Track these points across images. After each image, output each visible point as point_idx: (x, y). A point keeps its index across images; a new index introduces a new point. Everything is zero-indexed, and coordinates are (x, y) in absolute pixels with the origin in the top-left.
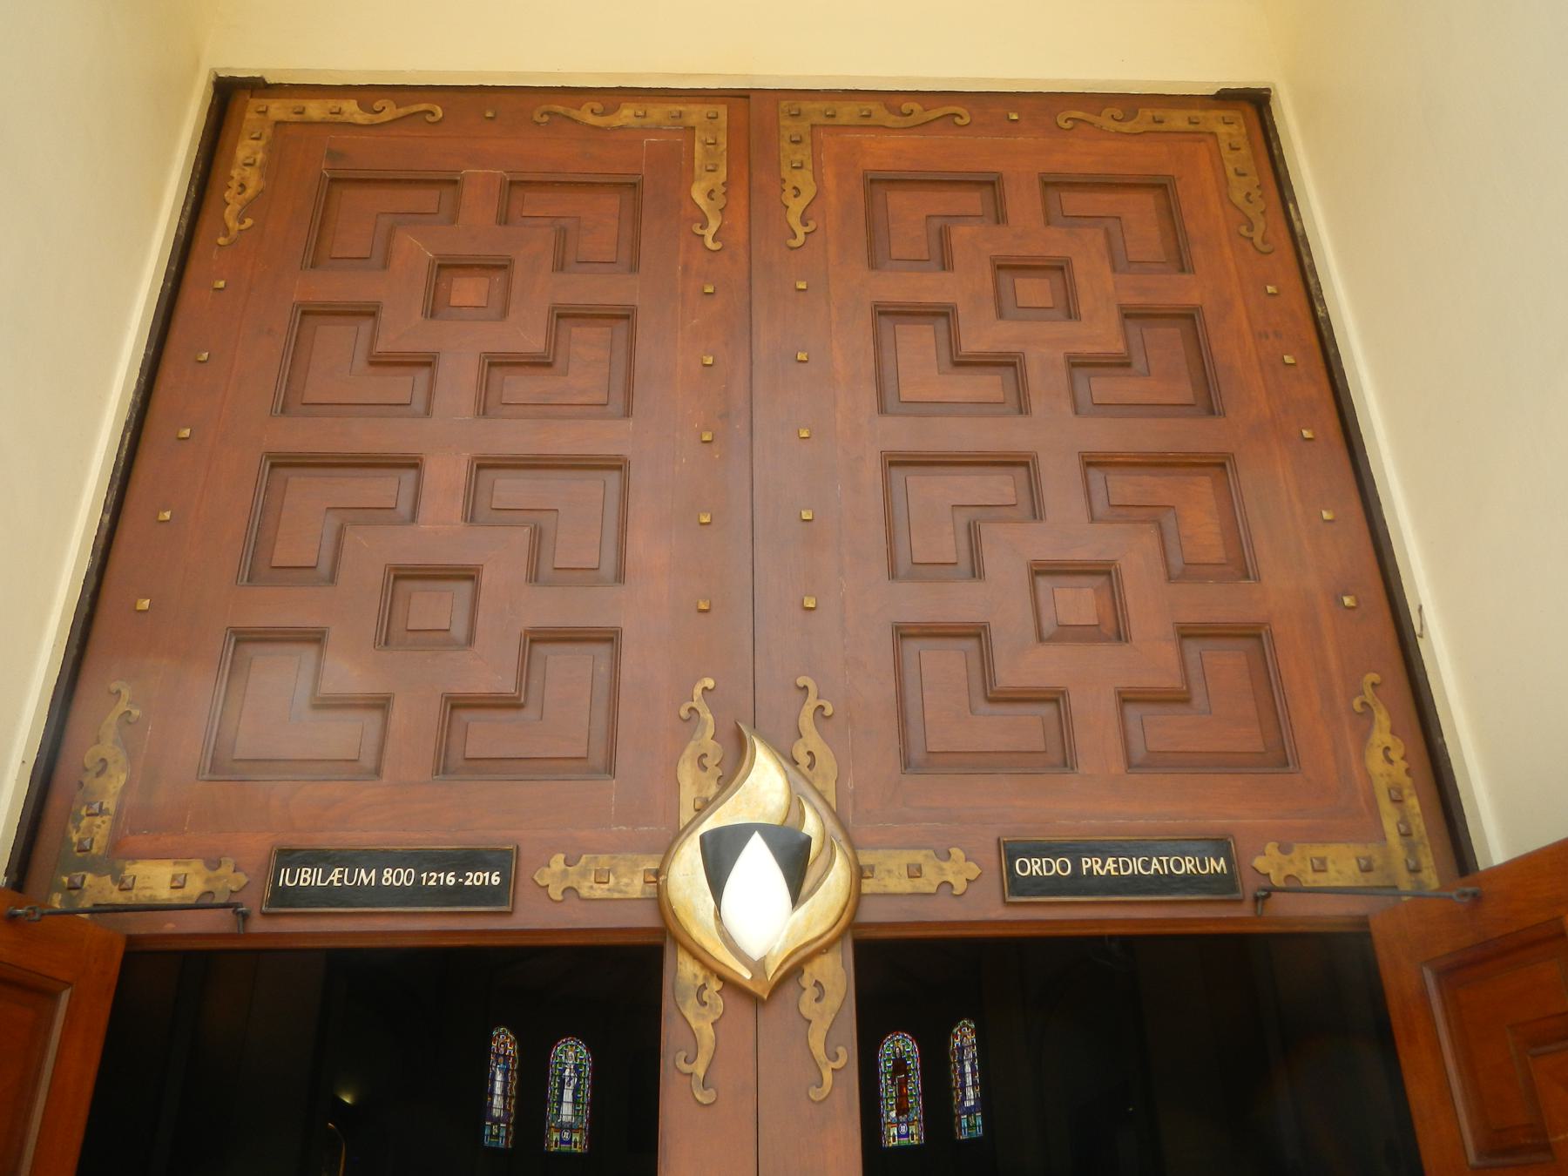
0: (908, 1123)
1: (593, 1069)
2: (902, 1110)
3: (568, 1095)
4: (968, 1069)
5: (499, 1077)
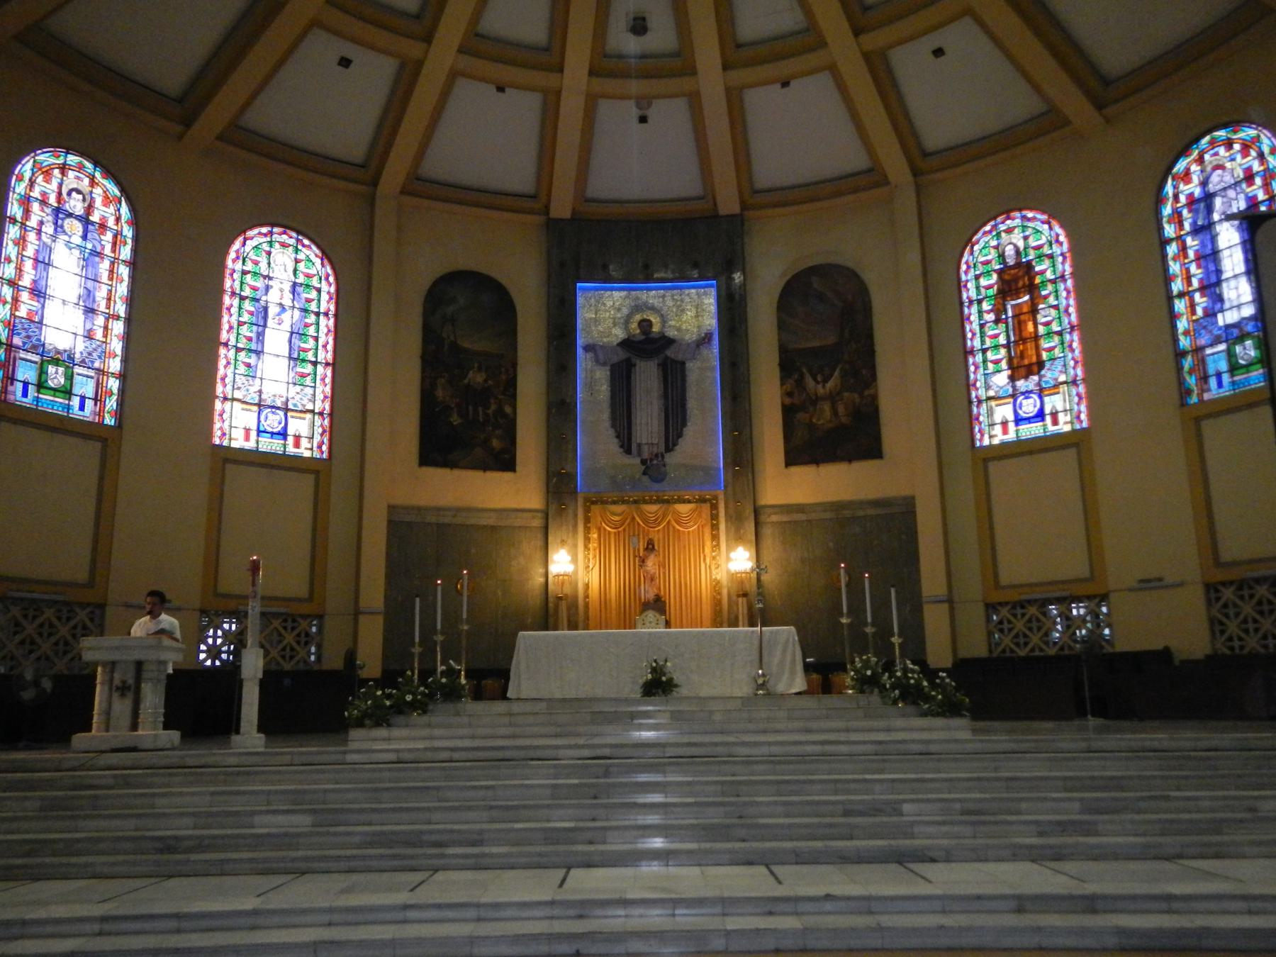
2: (1024, 363)
3: (276, 340)
5: (66, 260)
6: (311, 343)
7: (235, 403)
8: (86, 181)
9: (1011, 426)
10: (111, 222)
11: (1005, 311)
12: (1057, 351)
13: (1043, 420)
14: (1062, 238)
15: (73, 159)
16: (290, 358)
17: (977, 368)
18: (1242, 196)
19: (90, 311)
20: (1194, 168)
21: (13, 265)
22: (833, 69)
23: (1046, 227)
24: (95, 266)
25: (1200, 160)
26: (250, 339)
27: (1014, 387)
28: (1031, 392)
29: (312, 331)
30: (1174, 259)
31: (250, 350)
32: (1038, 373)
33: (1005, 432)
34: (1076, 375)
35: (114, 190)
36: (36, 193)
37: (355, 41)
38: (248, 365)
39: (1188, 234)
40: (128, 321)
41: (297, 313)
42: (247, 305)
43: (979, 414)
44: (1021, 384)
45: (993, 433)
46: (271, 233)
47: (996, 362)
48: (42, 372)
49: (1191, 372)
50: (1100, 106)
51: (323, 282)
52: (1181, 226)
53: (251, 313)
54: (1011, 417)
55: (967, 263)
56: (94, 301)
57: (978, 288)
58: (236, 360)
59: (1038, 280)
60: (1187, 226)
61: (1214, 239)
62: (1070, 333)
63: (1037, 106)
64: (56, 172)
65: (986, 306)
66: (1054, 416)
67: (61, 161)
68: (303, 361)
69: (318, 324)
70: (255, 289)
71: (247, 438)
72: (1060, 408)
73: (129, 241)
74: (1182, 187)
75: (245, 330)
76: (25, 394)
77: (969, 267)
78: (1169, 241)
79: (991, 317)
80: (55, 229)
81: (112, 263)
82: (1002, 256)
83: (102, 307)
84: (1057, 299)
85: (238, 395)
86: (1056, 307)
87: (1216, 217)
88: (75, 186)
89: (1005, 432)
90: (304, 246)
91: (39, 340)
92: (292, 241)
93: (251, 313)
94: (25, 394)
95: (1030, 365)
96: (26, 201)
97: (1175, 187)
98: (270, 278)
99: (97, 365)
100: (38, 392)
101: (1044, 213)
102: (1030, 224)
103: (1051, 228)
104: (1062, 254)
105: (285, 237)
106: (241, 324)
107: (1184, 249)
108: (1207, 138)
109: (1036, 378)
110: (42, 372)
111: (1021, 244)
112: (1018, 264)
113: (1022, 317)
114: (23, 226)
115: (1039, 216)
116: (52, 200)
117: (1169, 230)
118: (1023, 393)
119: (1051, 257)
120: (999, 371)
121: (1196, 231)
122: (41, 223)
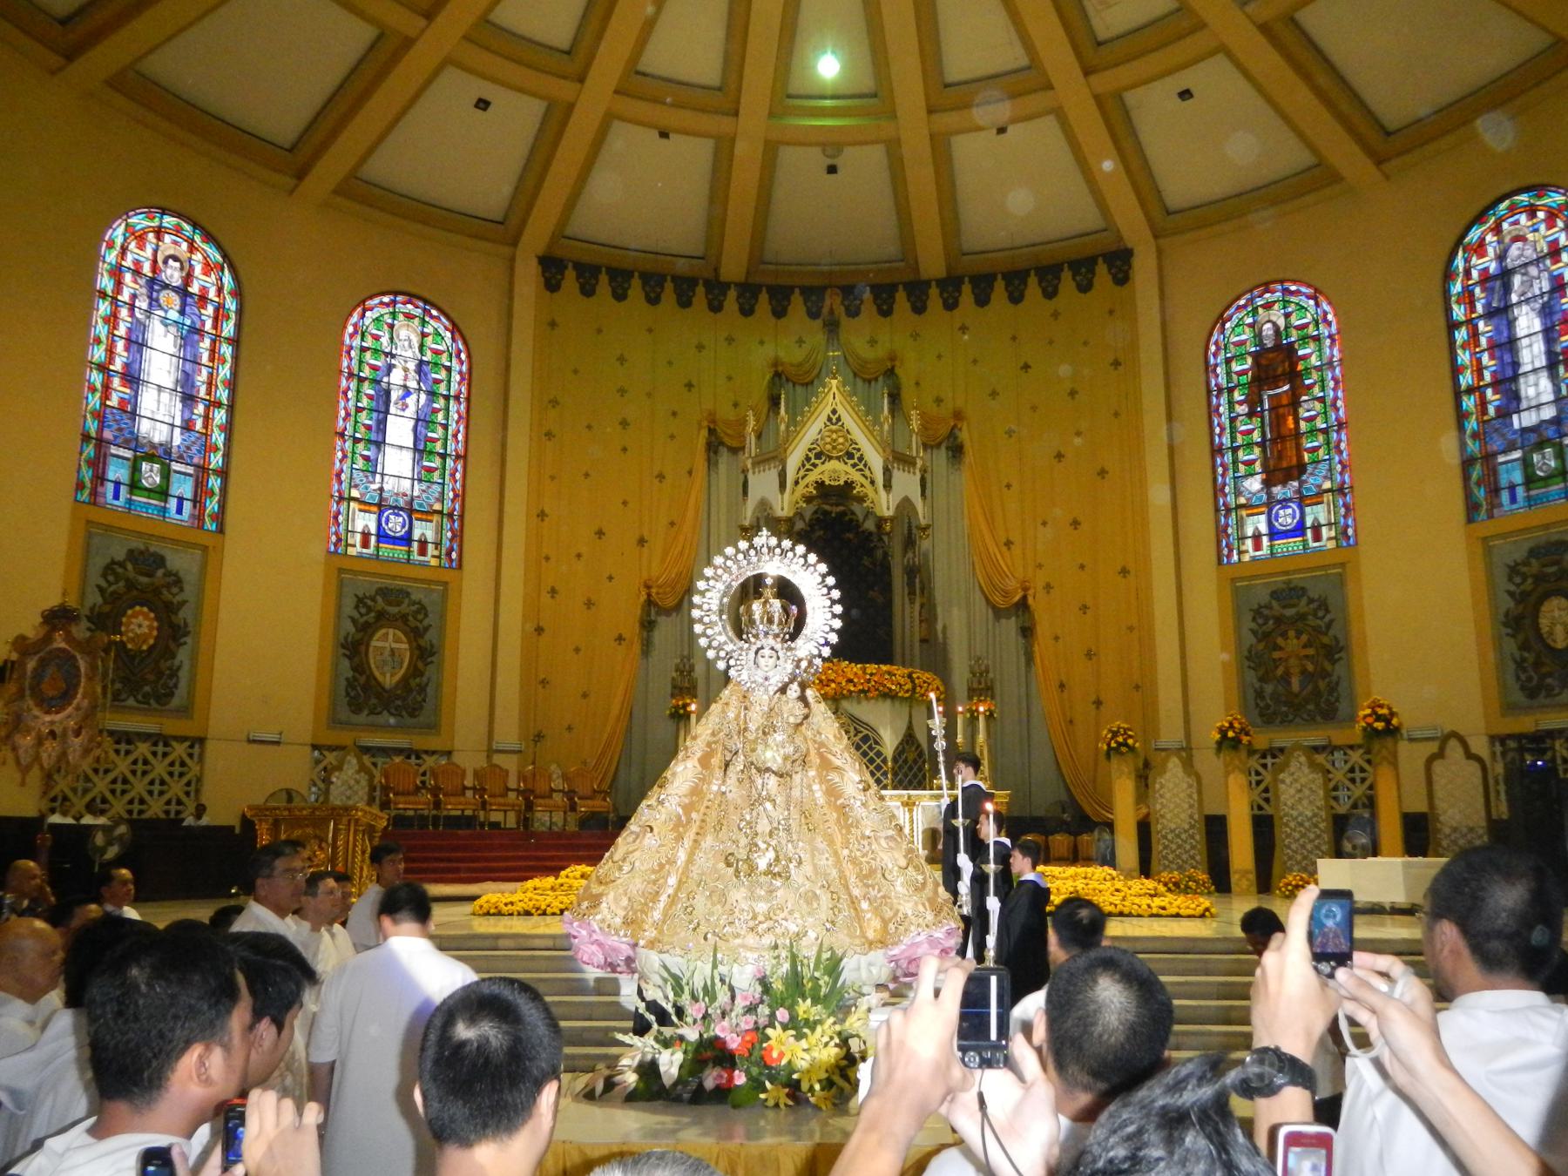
0: (1302, 501)
1: (468, 378)
2: (1283, 466)
3: (400, 429)
4: (1527, 322)
5: (162, 339)
6: (440, 430)
7: (352, 504)
8: (185, 246)
9: (1265, 541)
10: (212, 294)
11: (1262, 402)
12: (1321, 452)
13: (1303, 534)
14: (1330, 317)
15: (169, 221)
16: (415, 449)
17: (1225, 470)
18: (1546, 274)
19: (189, 399)
20: (1489, 238)
21: (103, 347)
22: (1059, 114)
23: (1312, 302)
24: (195, 345)
25: (1497, 229)
26: (369, 428)
27: (1269, 494)
28: (1290, 500)
29: (440, 417)
30: (1463, 347)
31: (370, 441)
32: (1298, 478)
33: (1258, 547)
34: (1344, 482)
35: (216, 256)
36: (128, 262)
37: (494, 80)
38: (366, 458)
39: (1480, 317)
40: (231, 409)
41: (423, 397)
42: (368, 389)
43: (1227, 525)
44: (1278, 491)
45: (1243, 548)
46: (394, 303)
47: (1249, 463)
48: (135, 470)
49: (1478, 484)
50: (1379, 162)
51: (454, 359)
52: (1473, 309)
53: (370, 397)
54: (1263, 528)
55: (1216, 343)
56: (193, 386)
57: (1229, 374)
58: (354, 453)
59: (1300, 367)
60: (1479, 308)
61: (1511, 323)
62: (1338, 432)
63: (1304, 158)
64: (151, 236)
65: (1238, 396)
66: (1317, 529)
67: (156, 223)
68: (431, 453)
69: (447, 409)
70: (374, 368)
71: (365, 544)
72: (1323, 521)
73: (233, 316)
74: (1474, 260)
75: (364, 418)
76: (116, 497)
77: (1218, 349)
78: (1458, 325)
79: (1243, 409)
80: (150, 305)
81: (213, 342)
82: (1258, 336)
83: (202, 393)
84: (1323, 390)
85: (355, 493)
86: (1322, 400)
87: (1514, 298)
88: (171, 252)
89: (1258, 547)
90: (432, 317)
91: (132, 433)
92: (418, 312)
93: (370, 397)
94: (116, 497)
95: (1290, 468)
96: (117, 273)
97: (1467, 261)
98: (393, 356)
99: (196, 460)
100: (131, 493)
101: (1309, 286)
102: (1293, 299)
103: (1317, 305)
104: (1330, 336)
105: (410, 306)
106: (359, 410)
107: (1475, 334)
108: (1506, 203)
109: (1296, 484)
110: (135, 470)
111: (1281, 322)
112: (1278, 347)
113: (1281, 411)
114: (115, 301)
115: (1303, 290)
116: (147, 269)
117: (1459, 312)
118: (1280, 502)
119: (1317, 339)
120: (1252, 475)
121: (1490, 314)
122: (134, 297)
